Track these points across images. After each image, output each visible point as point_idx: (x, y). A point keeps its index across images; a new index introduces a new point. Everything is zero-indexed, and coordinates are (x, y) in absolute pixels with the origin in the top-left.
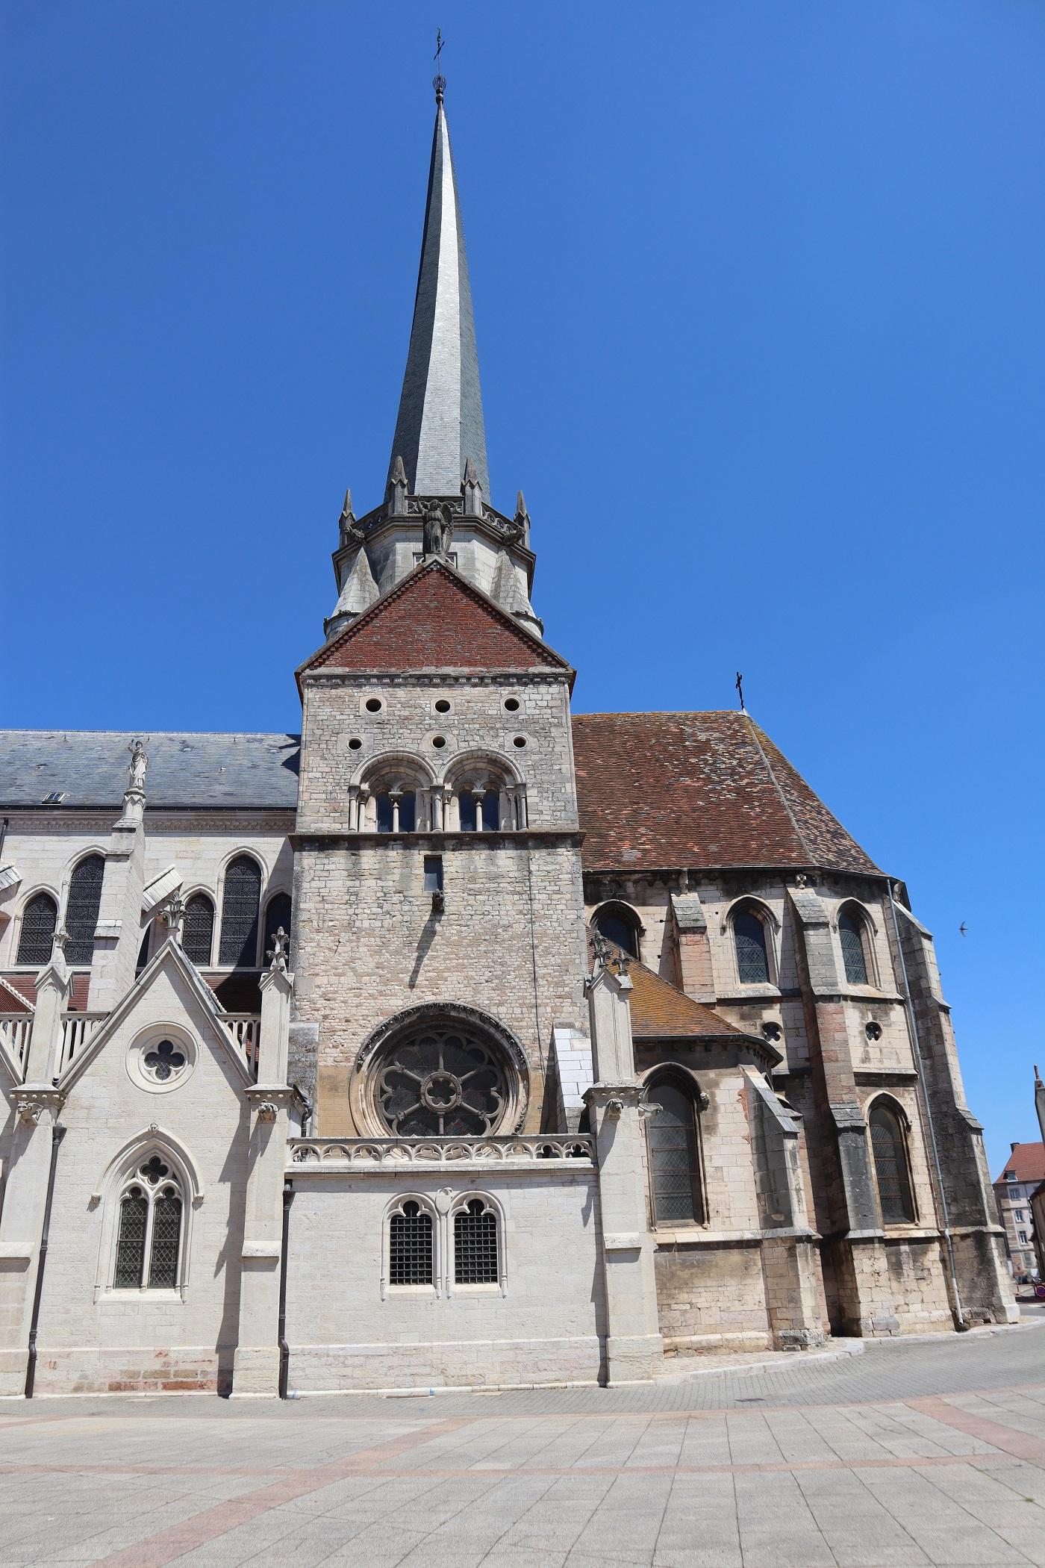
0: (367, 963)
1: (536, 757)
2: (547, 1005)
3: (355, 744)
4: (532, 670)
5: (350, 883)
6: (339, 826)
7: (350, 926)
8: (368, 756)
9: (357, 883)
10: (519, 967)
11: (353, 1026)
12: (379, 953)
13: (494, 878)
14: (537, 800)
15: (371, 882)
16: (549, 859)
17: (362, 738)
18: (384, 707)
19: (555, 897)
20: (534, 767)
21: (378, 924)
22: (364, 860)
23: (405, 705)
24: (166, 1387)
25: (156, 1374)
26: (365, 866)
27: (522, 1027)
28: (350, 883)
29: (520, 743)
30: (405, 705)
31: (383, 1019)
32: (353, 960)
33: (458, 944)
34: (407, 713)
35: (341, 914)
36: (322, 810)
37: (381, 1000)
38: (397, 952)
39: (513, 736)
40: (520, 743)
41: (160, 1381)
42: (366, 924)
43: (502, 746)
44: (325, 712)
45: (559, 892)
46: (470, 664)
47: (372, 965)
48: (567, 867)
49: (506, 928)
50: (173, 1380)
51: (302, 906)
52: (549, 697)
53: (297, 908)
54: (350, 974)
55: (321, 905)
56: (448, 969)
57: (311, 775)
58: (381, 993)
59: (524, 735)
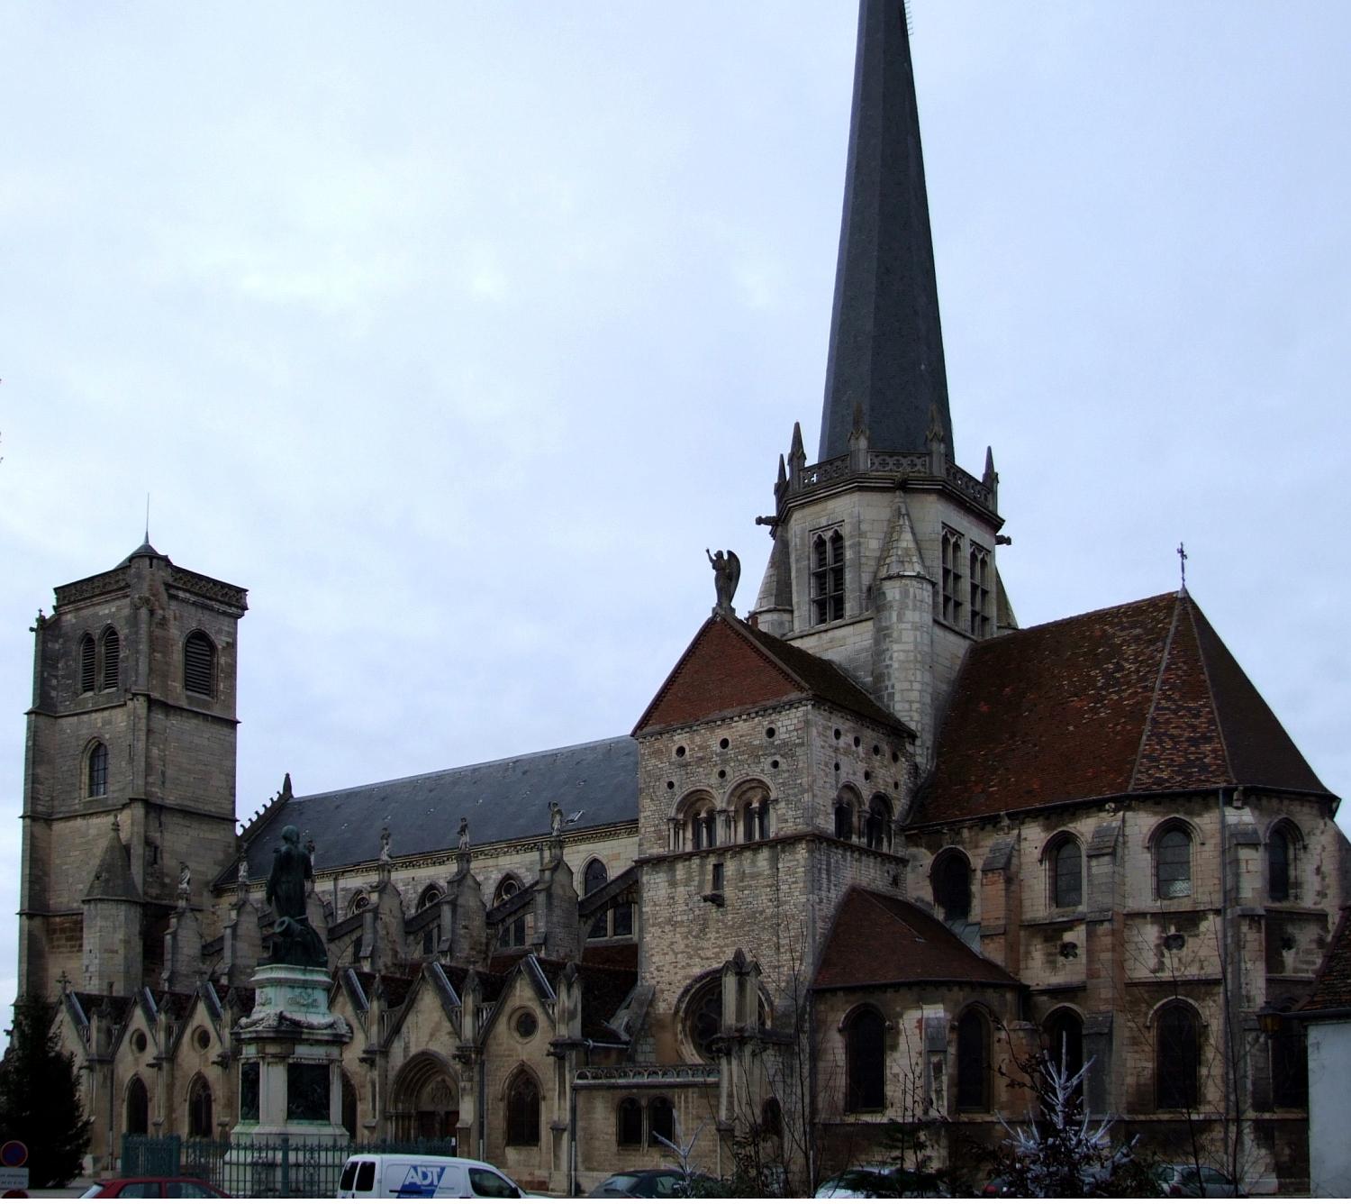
0: (680, 946)
1: (786, 775)
2: (783, 966)
3: (671, 785)
4: (785, 699)
5: (669, 891)
6: (662, 850)
7: (670, 921)
8: (680, 794)
10: (770, 940)
11: (673, 988)
12: (687, 938)
13: (754, 876)
14: (784, 811)
15: (681, 889)
16: (790, 858)
17: (674, 780)
18: (687, 752)
19: (793, 886)
20: (783, 784)
21: (685, 918)
22: (678, 873)
26: (678, 877)
27: (768, 982)
28: (669, 891)
29: (775, 764)
30: (701, 748)
31: (688, 981)
32: (672, 943)
33: (732, 927)
34: (700, 755)
35: (665, 913)
37: (688, 970)
38: (695, 937)
39: (770, 760)
40: (775, 764)
42: (679, 918)
43: (762, 771)
45: (796, 882)
46: (740, 703)
47: (683, 946)
48: (802, 862)
49: (762, 913)
52: (795, 721)
54: (671, 953)
56: (727, 946)
57: (645, 814)
58: (688, 965)
59: (777, 758)
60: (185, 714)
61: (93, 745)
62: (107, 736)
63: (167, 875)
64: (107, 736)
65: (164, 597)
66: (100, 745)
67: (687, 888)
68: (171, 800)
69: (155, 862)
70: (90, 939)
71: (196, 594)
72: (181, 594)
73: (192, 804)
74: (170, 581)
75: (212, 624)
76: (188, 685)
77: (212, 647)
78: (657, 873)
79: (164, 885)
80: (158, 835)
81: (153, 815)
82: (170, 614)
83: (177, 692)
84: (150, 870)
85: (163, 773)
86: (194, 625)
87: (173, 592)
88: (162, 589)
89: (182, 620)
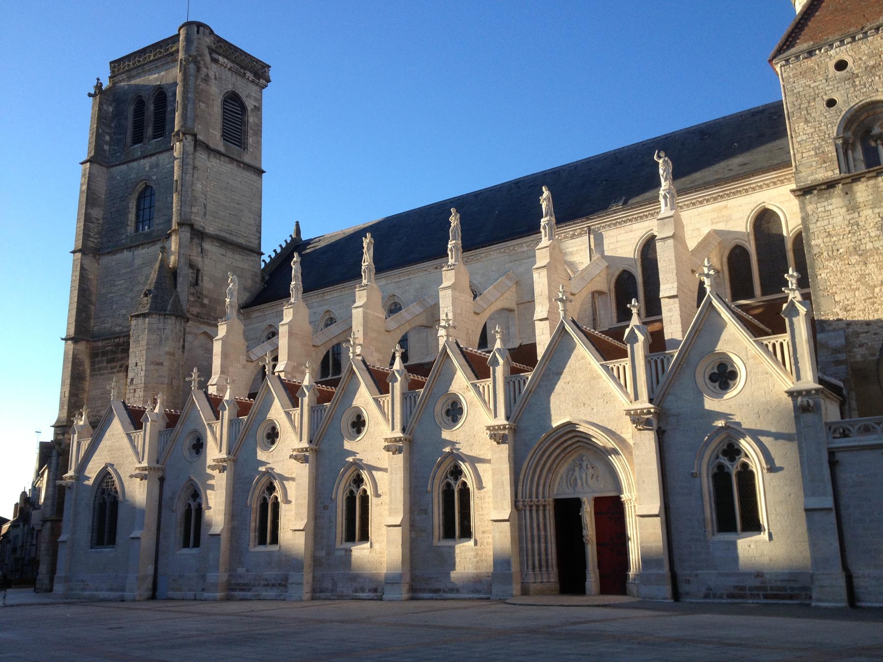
3: (831, 103)
5: (848, 217)
9: (856, 215)
18: (850, 64)
22: (859, 194)
23: (871, 56)
24: (766, 597)
25: (757, 588)
26: (860, 200)
32: (863, 276)
35: (845, 244)
36: (814, 164)
41: (761, 593)
42: (869, 246)
44: (800, 85)
50: (769, 592)
51: (813, 243)
53: (810, 246)
54: (862, 288)
55: (826, 240)
57: (799, 139)
60: (223, 158)
61: (140, 187)
62: (154, 178)
63: (206, 297)
64: (154, 178)
65: (208, 58)
66: (147, 187)
67: (877, 210)
68: (210, 230)
69: (197, 284)
70: (138, 356)
71: (233, 62)
72: (221, 59)
73: (227, 236)
74: (213, 47)
75: (245, 89)
76: (226, 136)
77: (243, 108)
78: (827, 199)
79: (203, 305)
80: (200, 259)
81: (196, 241)
82: (211, 74)
83: (215, 136)
84: (192, 290)
85: (205, 206)
86: (230, 88)
87: (215, 56)
88: (206, 52)
89: (220, 80)
